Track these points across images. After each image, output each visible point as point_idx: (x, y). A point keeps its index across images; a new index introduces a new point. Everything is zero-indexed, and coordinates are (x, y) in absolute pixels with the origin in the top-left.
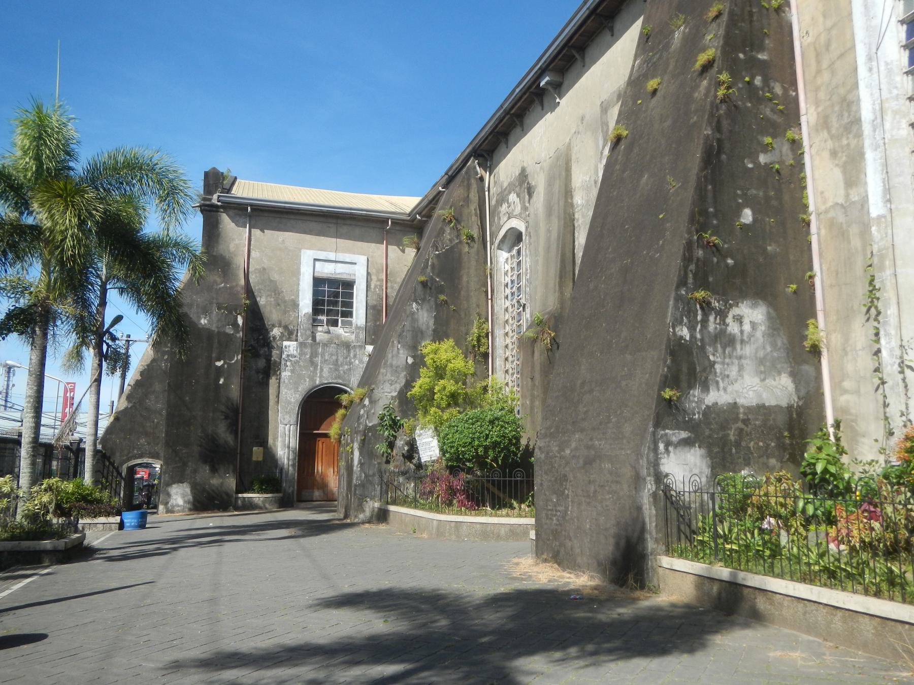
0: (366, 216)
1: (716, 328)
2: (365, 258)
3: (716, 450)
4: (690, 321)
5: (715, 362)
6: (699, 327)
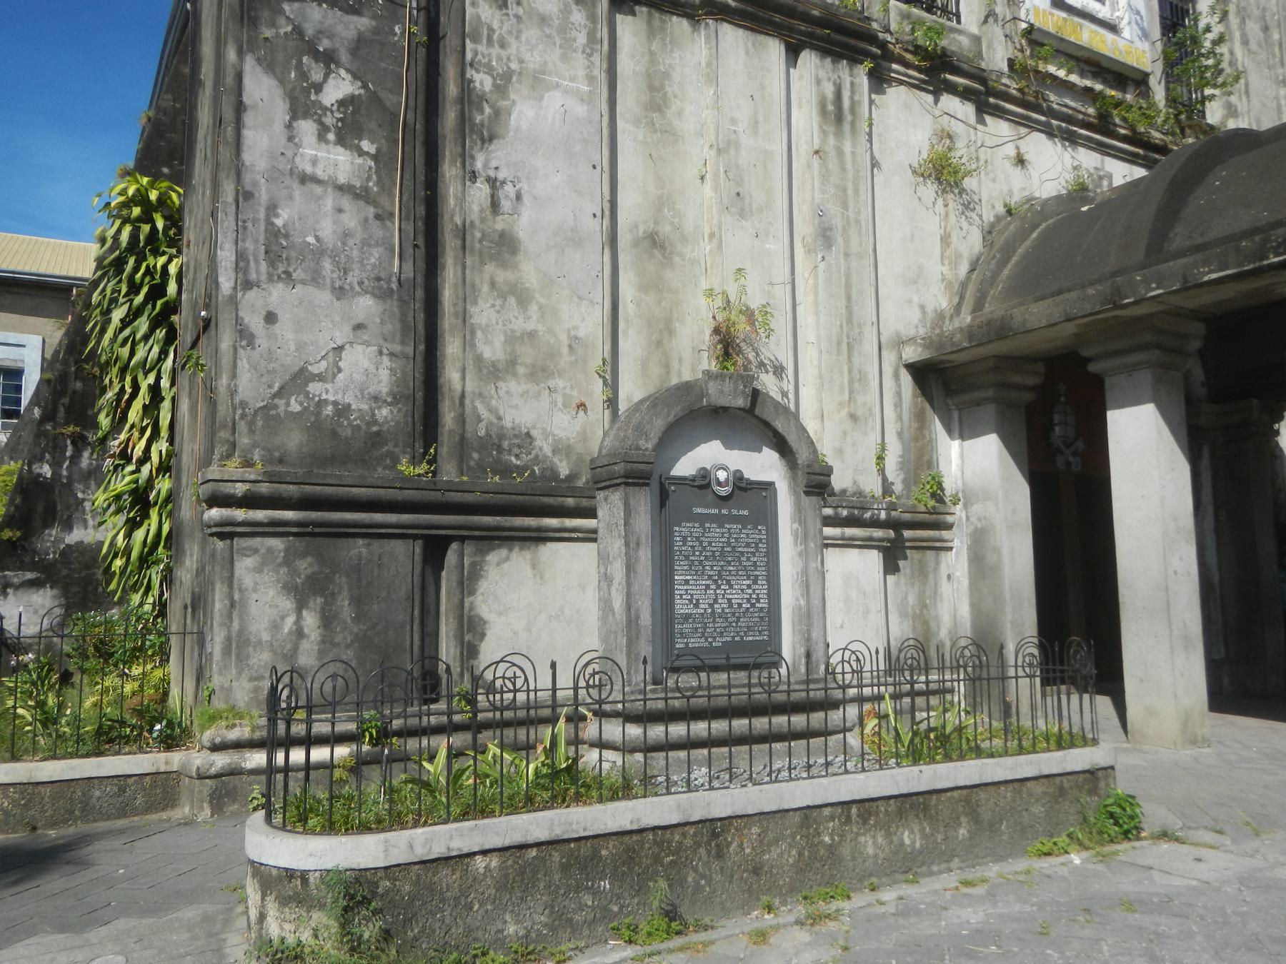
0: (37, 282)
1: (91, 464)
2: (40, 338)
3: (75, 589)
4: (54, 458)
5: (83, 500)
6: (67, 463)
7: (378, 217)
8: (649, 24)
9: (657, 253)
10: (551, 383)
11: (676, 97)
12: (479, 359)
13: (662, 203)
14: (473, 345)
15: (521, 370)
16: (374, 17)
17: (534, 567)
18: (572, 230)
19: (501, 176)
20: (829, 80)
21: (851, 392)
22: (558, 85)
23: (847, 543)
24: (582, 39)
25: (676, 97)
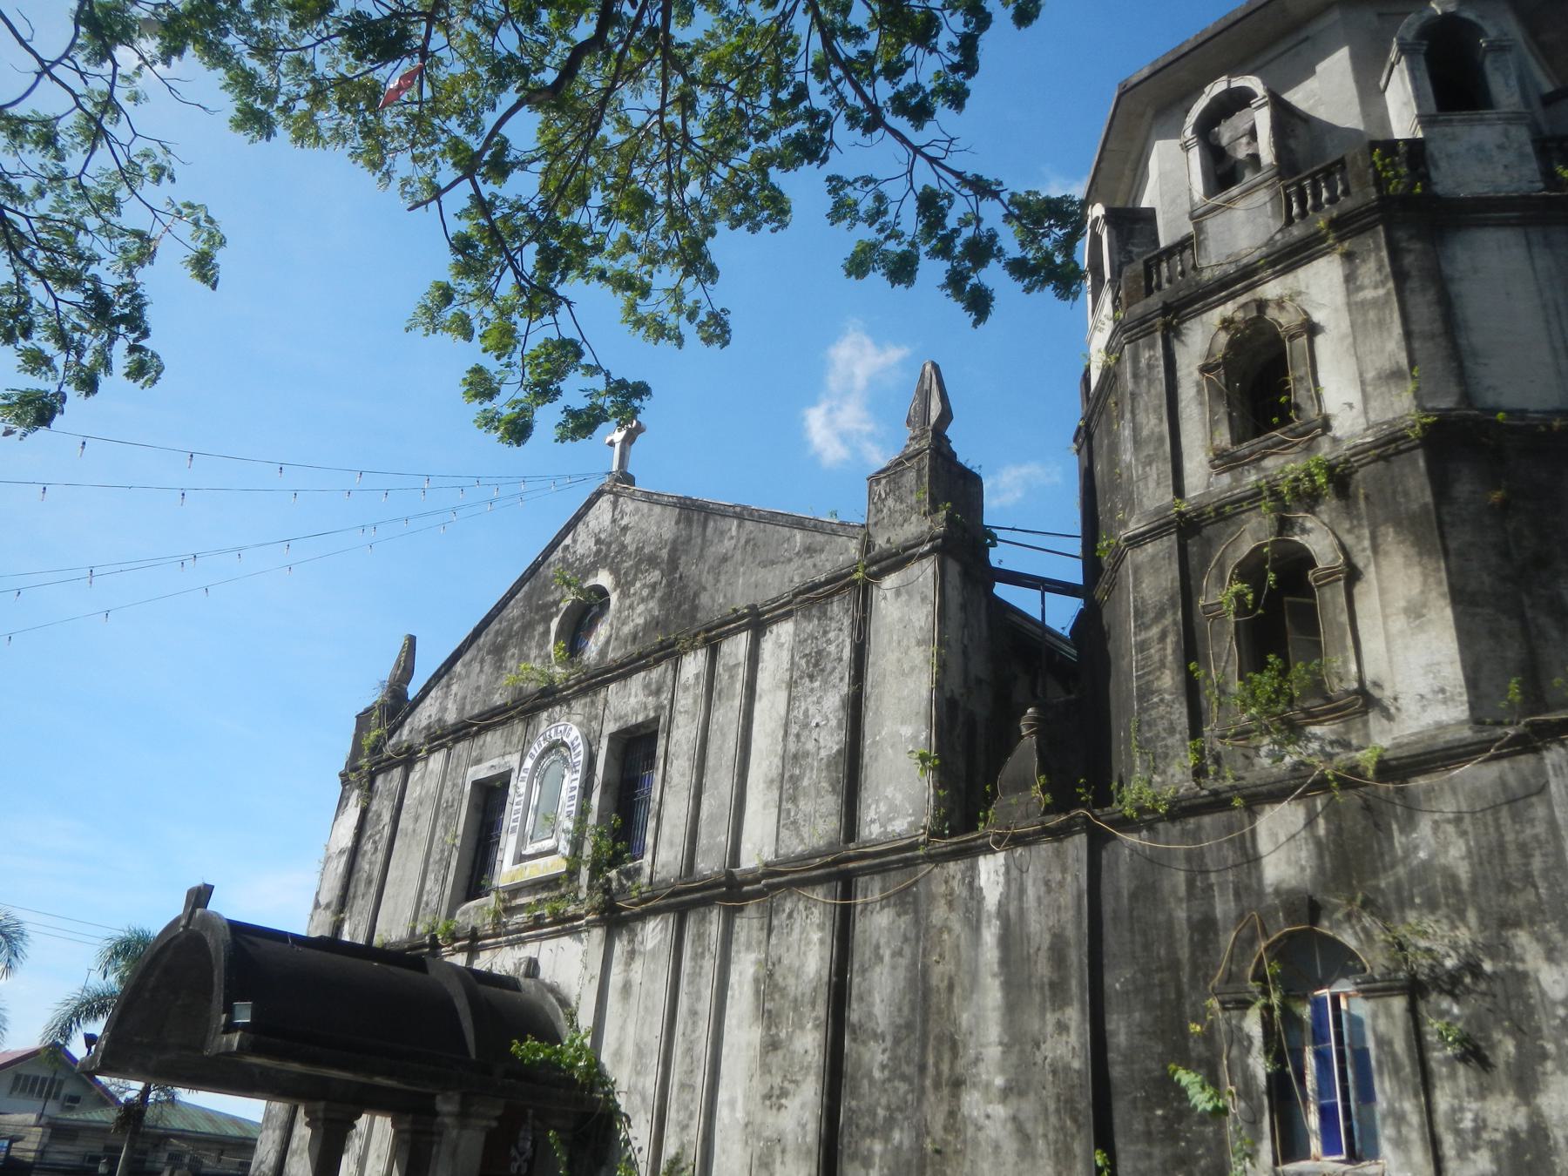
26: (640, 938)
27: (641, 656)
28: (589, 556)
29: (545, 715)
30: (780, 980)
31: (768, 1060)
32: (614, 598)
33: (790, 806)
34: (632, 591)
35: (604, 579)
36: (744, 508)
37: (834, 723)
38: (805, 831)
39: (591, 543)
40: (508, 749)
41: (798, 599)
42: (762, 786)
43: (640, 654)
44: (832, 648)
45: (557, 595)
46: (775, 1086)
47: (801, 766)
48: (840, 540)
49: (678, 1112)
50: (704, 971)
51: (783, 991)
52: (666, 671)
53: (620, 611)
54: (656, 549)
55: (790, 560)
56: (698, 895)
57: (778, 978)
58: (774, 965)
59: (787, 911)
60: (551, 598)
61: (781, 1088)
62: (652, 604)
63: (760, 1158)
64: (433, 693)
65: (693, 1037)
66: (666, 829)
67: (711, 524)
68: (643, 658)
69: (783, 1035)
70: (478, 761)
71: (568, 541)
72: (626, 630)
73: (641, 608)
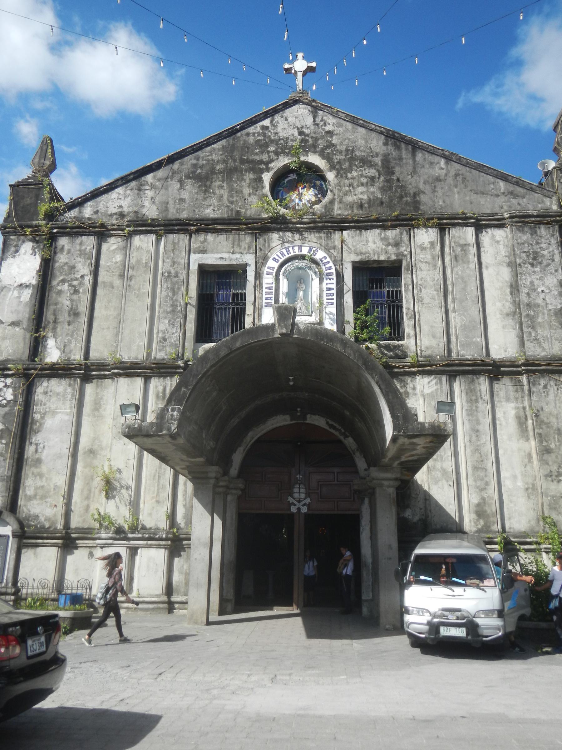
7: (4, 460)
8: (97, 384)
9: (92, 455)
10: (47, 500)
11: (104, 404)
12: (26, 495)
13: (96, 439)
14: (25, 491)
15: (38, 497)
16: (10, 407)
17: (35, 554)
18: (60, 454)
19: (39, 442)
20: (161, 385)
21: (158, 493)
22: (60, 412)
23: (150, 547)
24: (69, 396)
25: (104, 404)
26: (410, 385)
27: (378, 220)
28: (292, 140)
29: (275, 236)
30: (545, 419)
31: (544, 458)
32: (331, 176)
33: (530, 330)
34: (349, 175)
35: (314, 159)
36: (452, 154)
37: (556, 293)
38: (545, 345)
39: (296, 133)
40: (237, 249)
41: (514, 220)
42: (499, 316)
43: (378, 218)
44: (545, 252)
45: (265, 157)
46: (553, 470)
47: (534, 311)
48: (537, 195)
49: (475, 481)
50: (479, 409)
51: (548, 425)
52: (401, 234)
53: (339, 184)
54: (368, 155)
55: (498, 196)
56: (470, 368)
57: (543, 416)
58: (538, 411)
59: (542, 385)
60: (258, 158)
61: (558, 472)
62: (372, 189)
63: (549, 505)
64: (120, 190)
65: (478, 444)
66: (425, 328)
67: (419, 156)
68: (379, 221)
69: (553, 446)
70: (204, 251)
71: (266, 122)
72: (349, 199)
73: (361, 189)
